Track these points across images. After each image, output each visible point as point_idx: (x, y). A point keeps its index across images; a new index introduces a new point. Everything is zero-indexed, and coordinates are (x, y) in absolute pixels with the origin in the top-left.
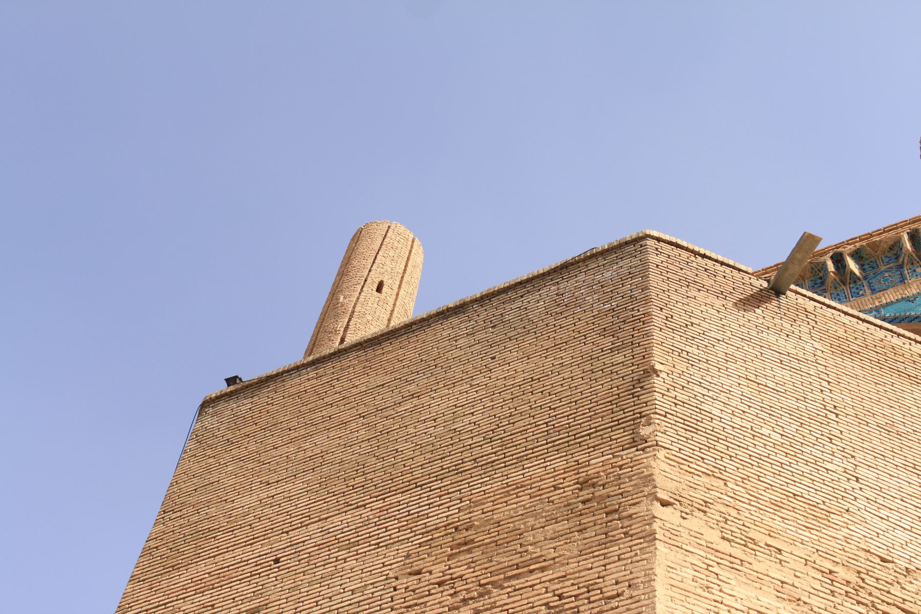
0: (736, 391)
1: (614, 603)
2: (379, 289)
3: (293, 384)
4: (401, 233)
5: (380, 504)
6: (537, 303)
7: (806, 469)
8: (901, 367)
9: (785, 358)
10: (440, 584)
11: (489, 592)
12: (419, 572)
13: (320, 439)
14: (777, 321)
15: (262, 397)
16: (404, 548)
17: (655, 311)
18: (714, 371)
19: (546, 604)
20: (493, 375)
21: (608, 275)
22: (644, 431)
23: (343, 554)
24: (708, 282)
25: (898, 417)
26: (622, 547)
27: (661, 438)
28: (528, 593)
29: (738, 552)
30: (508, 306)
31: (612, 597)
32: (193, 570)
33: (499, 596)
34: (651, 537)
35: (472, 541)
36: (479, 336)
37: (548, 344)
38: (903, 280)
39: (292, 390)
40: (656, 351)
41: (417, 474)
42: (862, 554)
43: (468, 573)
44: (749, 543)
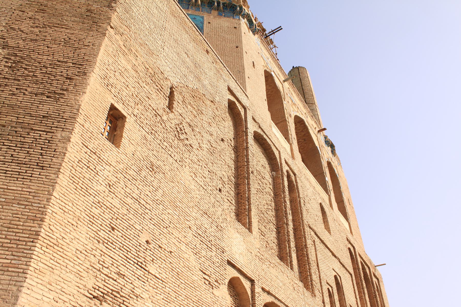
0: (142, 9)
1: (86, 47)
7: (152, 39)
8: (185, 27)
9: (158, 8)
10: (30, 18)
11: (46, 28)
12: (24, 12)
19: (64, 39)
22: (113, 5)
26: (95, 33)
27: (117, 9)
28: (60, 33)
29: (126, 51)
31: (86, 46)
34: (104, 35)
35: (46, 11)
43: (41, 19)
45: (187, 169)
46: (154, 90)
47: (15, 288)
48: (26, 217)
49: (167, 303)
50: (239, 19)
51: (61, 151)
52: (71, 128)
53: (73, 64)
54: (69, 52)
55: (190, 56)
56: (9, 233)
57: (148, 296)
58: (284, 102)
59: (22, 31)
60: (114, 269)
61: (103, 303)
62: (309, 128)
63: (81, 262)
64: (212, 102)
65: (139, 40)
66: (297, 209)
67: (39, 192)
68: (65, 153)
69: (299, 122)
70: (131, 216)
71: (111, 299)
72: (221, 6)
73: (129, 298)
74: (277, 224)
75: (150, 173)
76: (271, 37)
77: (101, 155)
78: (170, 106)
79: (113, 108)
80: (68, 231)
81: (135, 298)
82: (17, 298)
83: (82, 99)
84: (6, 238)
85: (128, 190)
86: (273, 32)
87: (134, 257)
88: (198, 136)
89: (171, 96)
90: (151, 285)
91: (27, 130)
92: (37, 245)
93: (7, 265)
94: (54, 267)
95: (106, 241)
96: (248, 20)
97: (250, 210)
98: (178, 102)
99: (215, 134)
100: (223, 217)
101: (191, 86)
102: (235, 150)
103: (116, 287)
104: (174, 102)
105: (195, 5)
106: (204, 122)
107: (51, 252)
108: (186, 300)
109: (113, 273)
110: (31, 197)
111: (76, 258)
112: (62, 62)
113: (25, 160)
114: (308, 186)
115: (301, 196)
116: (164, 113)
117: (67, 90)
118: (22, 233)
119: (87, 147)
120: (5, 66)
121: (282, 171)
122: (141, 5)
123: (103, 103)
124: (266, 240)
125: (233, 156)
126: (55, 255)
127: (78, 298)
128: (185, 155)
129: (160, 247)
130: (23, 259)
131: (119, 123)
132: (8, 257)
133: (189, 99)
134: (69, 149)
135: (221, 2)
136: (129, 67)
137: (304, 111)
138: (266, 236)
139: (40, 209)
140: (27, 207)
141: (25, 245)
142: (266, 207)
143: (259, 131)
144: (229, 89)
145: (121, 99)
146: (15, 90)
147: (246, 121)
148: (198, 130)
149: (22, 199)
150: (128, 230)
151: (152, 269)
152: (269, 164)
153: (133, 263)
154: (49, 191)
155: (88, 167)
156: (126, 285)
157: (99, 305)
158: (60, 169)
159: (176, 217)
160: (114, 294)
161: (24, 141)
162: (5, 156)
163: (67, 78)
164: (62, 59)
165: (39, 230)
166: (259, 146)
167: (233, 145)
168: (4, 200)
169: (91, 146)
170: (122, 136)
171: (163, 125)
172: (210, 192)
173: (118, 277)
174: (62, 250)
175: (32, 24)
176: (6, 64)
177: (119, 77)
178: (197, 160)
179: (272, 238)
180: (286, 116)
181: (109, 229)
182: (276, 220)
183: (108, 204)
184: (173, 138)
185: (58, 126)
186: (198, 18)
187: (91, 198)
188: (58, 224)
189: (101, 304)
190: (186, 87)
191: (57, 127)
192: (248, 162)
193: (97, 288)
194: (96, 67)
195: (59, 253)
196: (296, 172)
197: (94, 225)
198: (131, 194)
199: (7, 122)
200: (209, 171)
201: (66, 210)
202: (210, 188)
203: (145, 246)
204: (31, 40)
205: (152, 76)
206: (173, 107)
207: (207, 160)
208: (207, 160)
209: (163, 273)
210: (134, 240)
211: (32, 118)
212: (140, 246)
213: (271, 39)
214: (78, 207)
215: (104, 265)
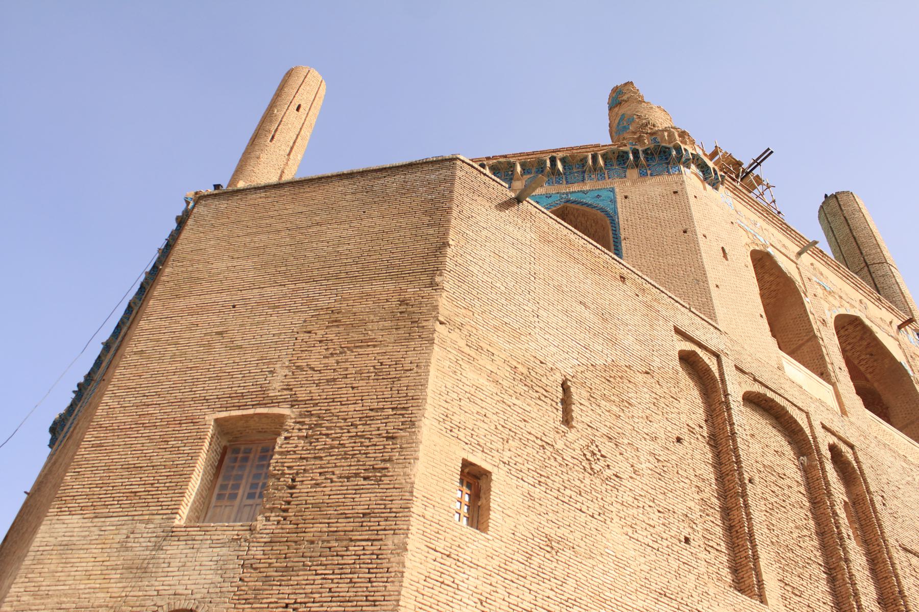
0: (488, 260)
1: (408, 374)
2: (298, 109)
3: (253, 198)
4: (315, 77)
5: (293, 286)
6: (393, 182)
7: (514, 308)
8: (571, 251)
10: (320, 342)
11: (345, 352)
12: (310, 332)
13: (264, 237)
14: (515, 219)
15: (234, 202)
17: (454, 207)
19: (374, 366)
21: (433, 177)
22: (438, 279)
24: (484, 191)
25: (565, 282)
27: (446, 285)
29: (473, 353)
32: (187, 300)
33: (350, 356)
34: (432, 341)
35: (340, 321)
36: (359, 196)
37: (395, 211)
38: (583, 180)
39: (251, 202)
40: (451, 232)
41: (315, 273)
42: (532, 359)
43: (336, 339)
44: (479, 349)
45: (615, 526)
50: (680, 173)
51: (396, 569)
52: (405, 527)
53: (393, 409)
55: (589, 305)
58: (806, 300)
59: (313, 369)
62: (875, 329)
66: (868, 518)
68: (403, 572)
69: (851, 328)
74: (827, 563)
75: (548, 556)
76: (755, 172)
77: (460, 555)
78: (567, 420)
79: (466, 464)
83: (415, 470)
85: (513, 600)
86: (757, 163)
89: (567, 401)
91: (345, 543)
96: (698, 166)
97: (756, 558)
98: (581, 404)
100: (700, 590)
101: (600, 362)
102: (712, 443)
104: (573, 407)
105: (595, 170)
106: (637, 420)
112: (376, 410)
113: (348, 594)
114: (886, 457)
115: (872, 489)
116: (557, 436)
117: (390, 460)
119: (435, 550)
120: (299, 438)
121: (818, 451)
122: (483, 253)
123: (449, 464)
124: (806, 602)
125: (710, 455)
128: (608, 499)
131: (482, 483)
133: (601, 387)
134: (407, 564)
135: (640, 149)
136: (483, 381)
137: (856, 296)
138: (806, 595)
142: (795, 535)
143: (757, 388)
144: (678, 331)
145: (478, 445)
146: (317, 476)
147: (723, 380)
148: (626, 441)
152: (790, 443)
155: (442, 583)
158: (398, 601)
161: (343, 562)
162: (321, 593)
163: (388, 438)
164: (375, 405)
166: (762, 416)
167: (705, 434)
169: (440, 546)
170: (489, 509)
171: (559, 459)
175: (324, 352)
176: (301, 434)
178: (631, 499)
179: (820, 596)
180: (815, 327)
182: (822, 555)
185: (387, 528)
186: (604, 194)
190: (591, 368)
191: (385, 530)
192: (738, 462)
194: (427, 407)
196: (852, 440)
198: (520, 605)
199: (316, 534)
200: (659, 512)
202: (665, 543)
204: (328, 381)
206: (572, 418)
207: (653, 492)
208: (653, 492)
211: (349, 520)
213: (758, 176)
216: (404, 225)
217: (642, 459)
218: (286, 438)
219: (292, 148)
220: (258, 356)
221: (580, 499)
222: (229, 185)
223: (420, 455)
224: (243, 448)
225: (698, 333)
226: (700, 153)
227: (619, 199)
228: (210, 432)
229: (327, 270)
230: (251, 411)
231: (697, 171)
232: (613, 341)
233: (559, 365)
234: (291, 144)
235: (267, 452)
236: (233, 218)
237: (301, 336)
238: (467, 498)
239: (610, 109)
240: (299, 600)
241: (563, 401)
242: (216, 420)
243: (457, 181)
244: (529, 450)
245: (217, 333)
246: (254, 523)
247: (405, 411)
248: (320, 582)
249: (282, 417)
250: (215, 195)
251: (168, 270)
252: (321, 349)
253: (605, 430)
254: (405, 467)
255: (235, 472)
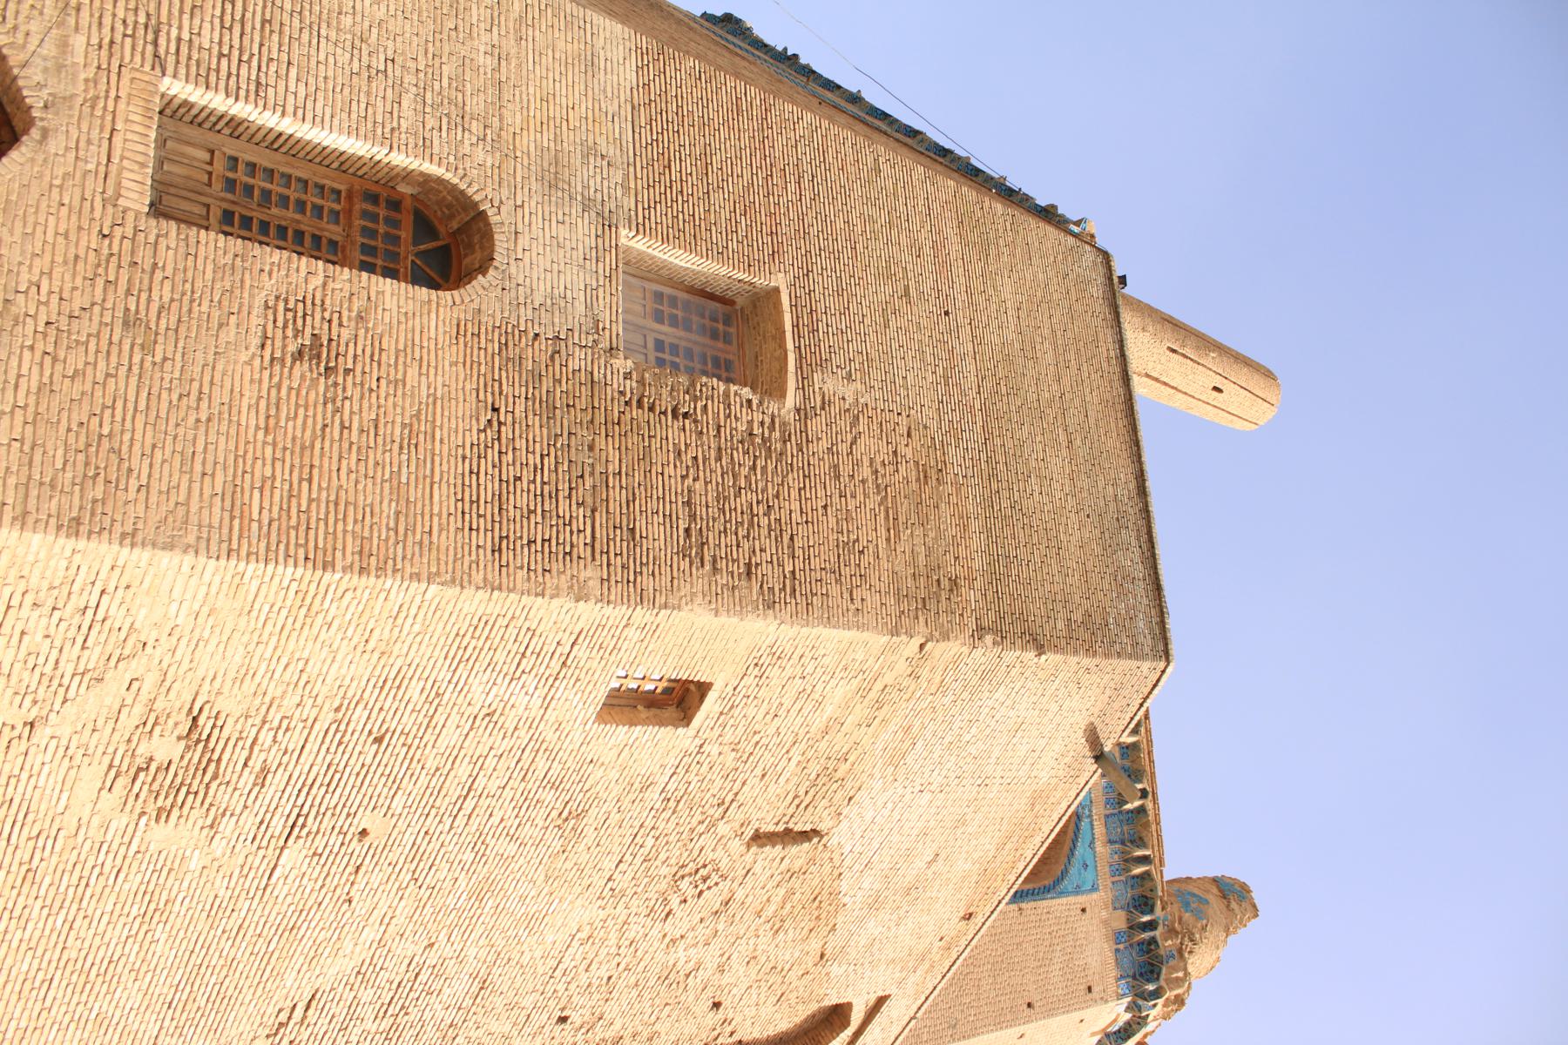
0: (1012, 713)
2: (1216, 389)
3: (1108, 337)
4: (1263, 414)
6: (1132, 561)
7: (936, 756)
8: (1014, 839)
9: (1036, 754)
10: (895, 452)
12: (909, 435)
13: (1050, 357)
15: (1101, 308)
16: (933, 425)
17: (1096, 661)
18: (1034, 699)
20: (1072, 515)
21: (1141, 624)
22: (989, 639)
23: (940, 371)
24: (1116, 705)
25: (970, 830)
26: (893, 609)
27: (978, 653)
28: (871, 525)
29: (873, 695)
30: (1133, 534)
32: (955, 239)
33: (873, 501)
34: (895, 632)
36: (1112, 505)
37: (1089, 565)
38: (1111, 842)
39: (1101, 335)
40: (1059, 657)
41: (998, 441)
44: (879, 704)
45: (595, 913)
46: (790, 786)
47: (191, 539)
48: (366, 534)
49: (208, 907)
50: (1120, 997)
52: (612, 598)
53: (793, 572)
54: (827, 555)
55: (933, 868)
56: (323, 505)
57: (218, 853)
60: (274, 758)
61: (183, 743)
63: (276, 676)
64: (822, 956)
65: (918, 724)
67: (434, 552)
70: (423, 781)
71: (195, 760)
72: (1146, 935)
73: (206, 806)
75: (554, 814)
78: (759, 839)
79: (703, 688)
80: (349, 633)
81: (209, 822)
82: (169, 547)
83: (699, 610)
84: (310, 500)
87: (317, 802)
88: (703, 932)
89: (789, 837)
90: (250, 858)
91: (589, 500)
92: (300, 570)
93: (247, 514)
94: (254, 614)
95: (342, 727)
96: (1128, 1023)
99: (726, 979)
101: (844, 885)
103: (230, 769)
104: (779, 847)
105: (1126, 861)
106: (752, 942)
107: (288, 603)
108: (222, 962)
109: (263, 756)
110: (418, 537)
111: (284, 661)
112: (792, 546)
113: (511, 508)
116: (737, 825)
117: (715, 570)
118: (327, 533)
120: (750, 422)
126: (284, 612)
127: (187, 681)
128: (635, 902)
129: (358, 868)
130: (263, 545)
131: (671, 712)
132: (265, 512)
134: (556, 602)
135: (1157, 933)
136: (829, 710)
139: (390, 562)
140: (392, 533)
141: (297, 545)
144: (881, 1001)
148: (721, 927)
149: (411, 519)
150: (384, 779)
151: (294, 855)
153: (300, 802)
154: (438, 574)
156: (237, 793)
157: (176, 733)
159: (451, 901)
160: (210, 765)
163: (749, 565)
164: (798, 543)
165: (339, 566)
168: (404, 480)
169: (580, 652)
171: (702, 828)
172: (550, 989)
173: (257, 769)
174: (298, 626)
175: (878, 460)
177: (791, 692)
178: (631, 937)
181: (375, 730)
183: (439, 718)
184: (673, 861)
186: (1089, 875)
187: (444, 675)
188: (361, 607)
189: (179, 738)
190: (836, 873)
191: (609, 565)
193: (220, 723)
194: (796, 628)
195: (290, 620)
197: (377, 691)
201: (400, 621)
202: (561, 987)
203: (352, 829)
204: (836, 467)
205: (827, 773)
206: (762, 846)
209: (286, 888)
210: (360, 796)
212: (348, 815)
214: (415, 647)
215: (281, 732)
216: (1069, 580)
217: (692, 951)
218: (749, 401)
219: (1157, 380)
220: (874, 355)
221: (638, 860)
222: (1124, 296)
223: (723, 619)
224: (732, 330)
225: (878, 1030)
226: (1149, 1028)
227: (1082, 899)
228: (761, 281)
229: (1002, 459)
230: (790, 345)
231: (1120, 1023)
232: (875, 904)
233: (845, 824)
234: (1163, 379)
235: (724, 370)
236: (1078, 307)
237: (903, 421)
238: (650, 687)
239: (1215, 880)
240: (503, 428)
241: (788, 831)
242: (777, 290)
243: (1133, 663)
244: (719, 782)
245: (907, 288)
246: (621, 355)
247: (790, 592)
248: (531, 462)
249: (783, 395)
250: (1110, 279)
251: (999, 207)
252: (884, 454)
253: (740, 894)
254: (704, 596)
255: (695, 318)
